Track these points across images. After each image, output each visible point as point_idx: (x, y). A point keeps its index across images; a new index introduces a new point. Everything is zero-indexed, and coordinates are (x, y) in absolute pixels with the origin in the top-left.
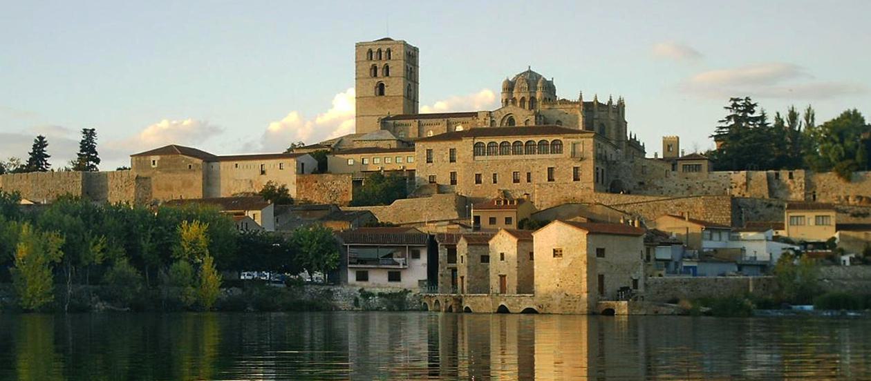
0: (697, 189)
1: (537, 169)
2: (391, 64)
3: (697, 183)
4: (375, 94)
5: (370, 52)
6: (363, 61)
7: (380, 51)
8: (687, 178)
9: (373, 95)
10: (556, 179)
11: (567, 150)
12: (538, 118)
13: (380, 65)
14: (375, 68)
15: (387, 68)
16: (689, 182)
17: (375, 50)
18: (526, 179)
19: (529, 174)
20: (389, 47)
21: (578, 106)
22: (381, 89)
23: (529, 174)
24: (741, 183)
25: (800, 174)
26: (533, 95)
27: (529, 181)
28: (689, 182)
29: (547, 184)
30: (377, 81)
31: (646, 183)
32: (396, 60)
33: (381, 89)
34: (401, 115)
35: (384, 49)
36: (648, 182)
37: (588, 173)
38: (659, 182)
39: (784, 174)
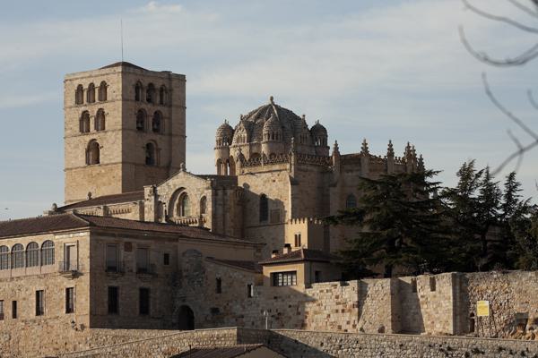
0: (290, 318)
1: (23, 294)
2: (107, 107)
3: (290, 306)
4: (88, 162)
5: (80, 89)
6: (71, 107)
7: (92, 86)
8: (275, 298)
9: (84, 164)
10: (46, 310)
11: (59, 256)
12: (220, 193)
13: (93, 110)
14: (85, 117)
15: (101, 115)
16: (278, 304)
17: (86, 87)
18: (10, 312)
19: (15, 303)
20: (104, 78)
21: (288, 166)
22: (93, 151)
23: (15, 303)
24: (351, 303)
25: (445, 282)
26: (255, 150)
27: (15, 316)
28: (278, 304)
29: (35, 321)
30: (88, 138)
31: (222, 310)
32: (113, 101)
33: (93, 151)
34: (119, 196)
35: (97, 84)
36: (225, 307)
37: (83, 300)
38: (238, 306)
39: (423, 280)
